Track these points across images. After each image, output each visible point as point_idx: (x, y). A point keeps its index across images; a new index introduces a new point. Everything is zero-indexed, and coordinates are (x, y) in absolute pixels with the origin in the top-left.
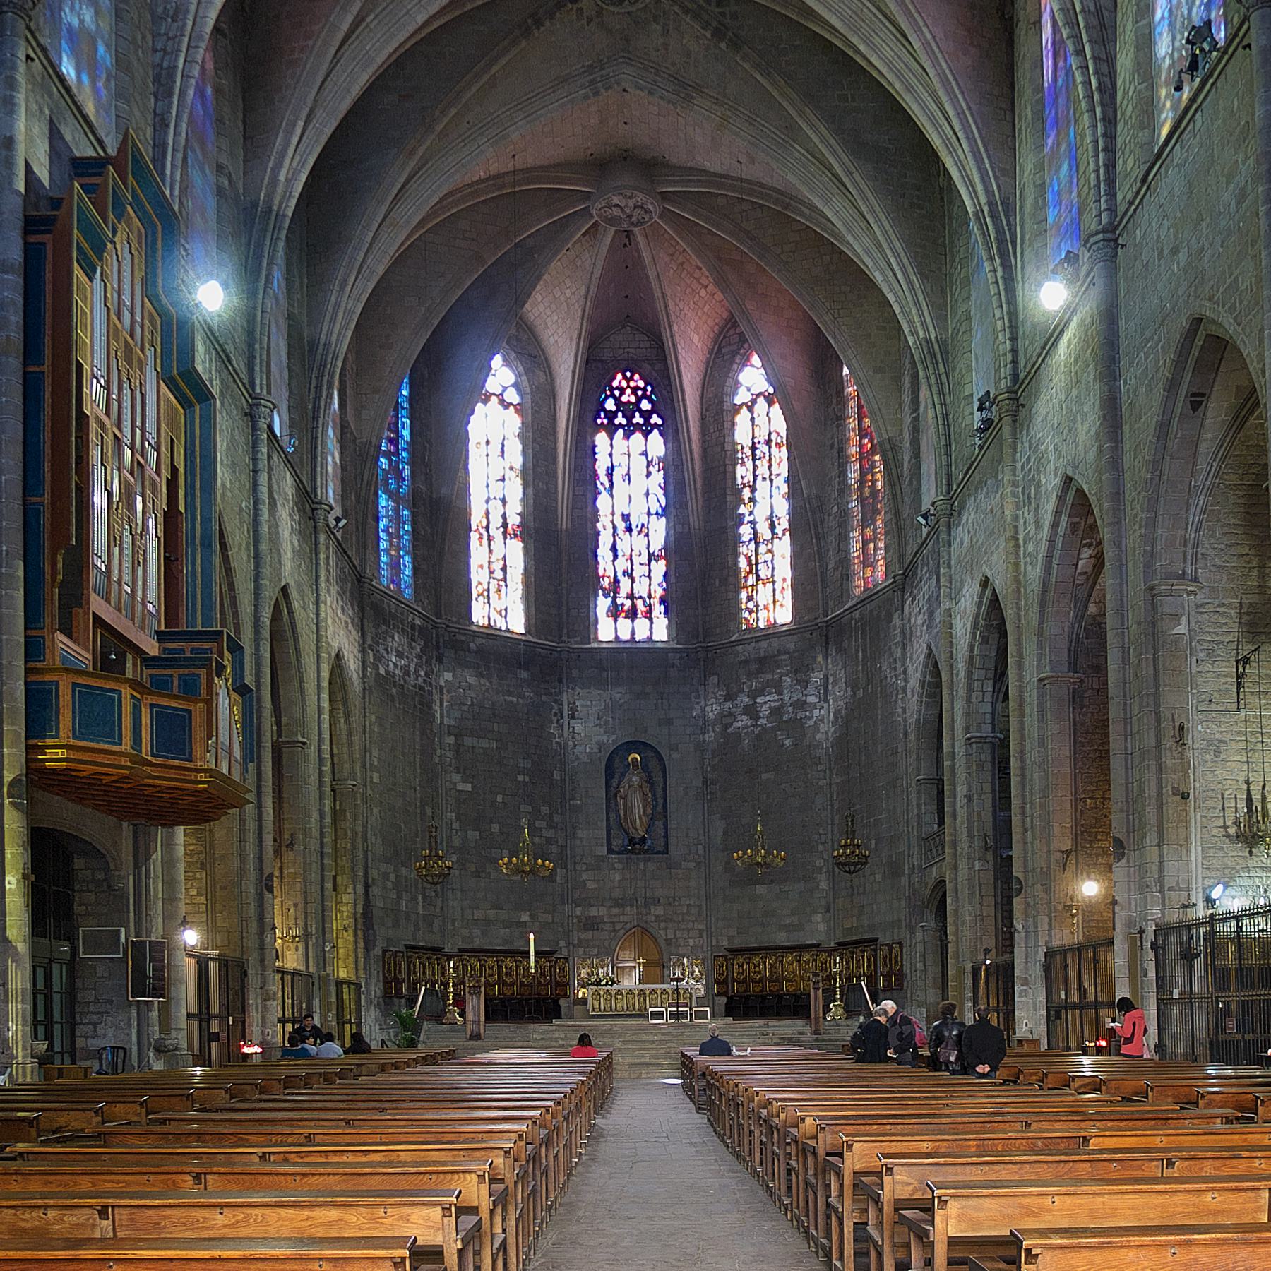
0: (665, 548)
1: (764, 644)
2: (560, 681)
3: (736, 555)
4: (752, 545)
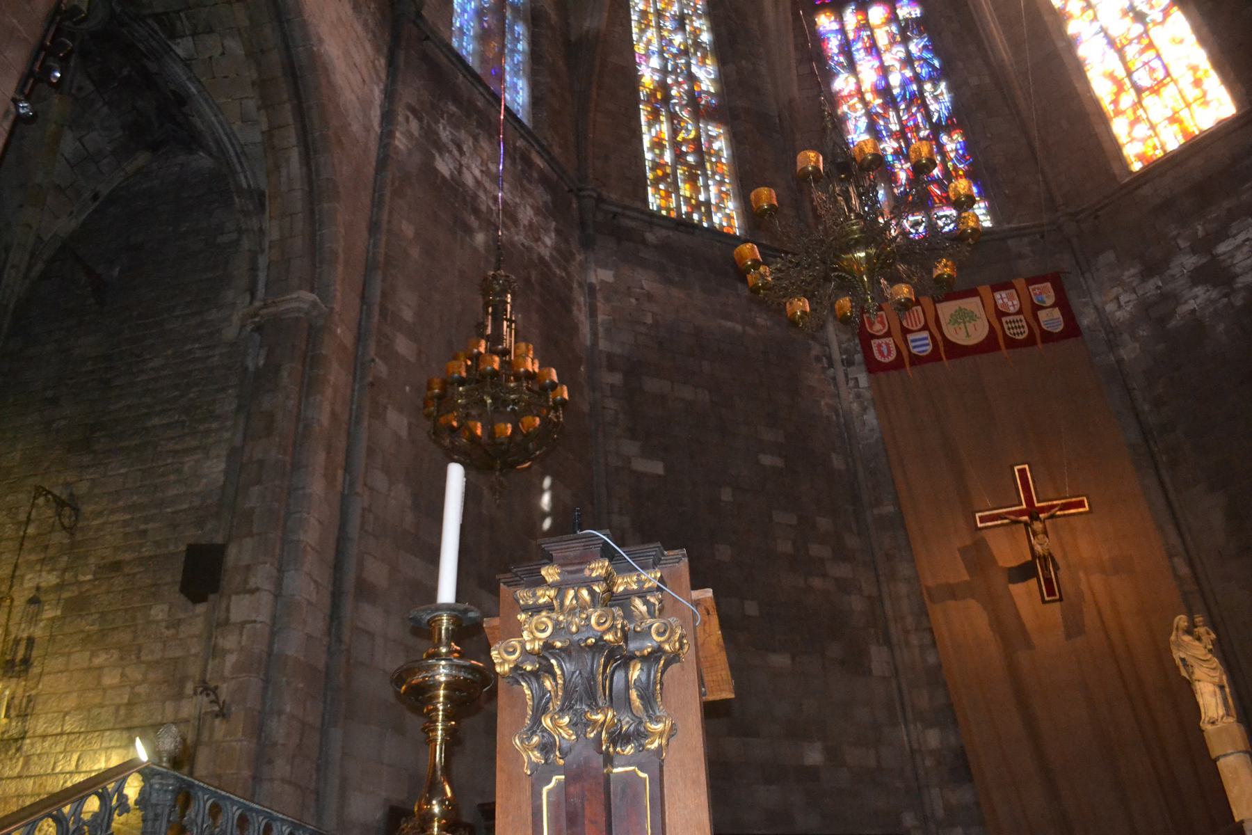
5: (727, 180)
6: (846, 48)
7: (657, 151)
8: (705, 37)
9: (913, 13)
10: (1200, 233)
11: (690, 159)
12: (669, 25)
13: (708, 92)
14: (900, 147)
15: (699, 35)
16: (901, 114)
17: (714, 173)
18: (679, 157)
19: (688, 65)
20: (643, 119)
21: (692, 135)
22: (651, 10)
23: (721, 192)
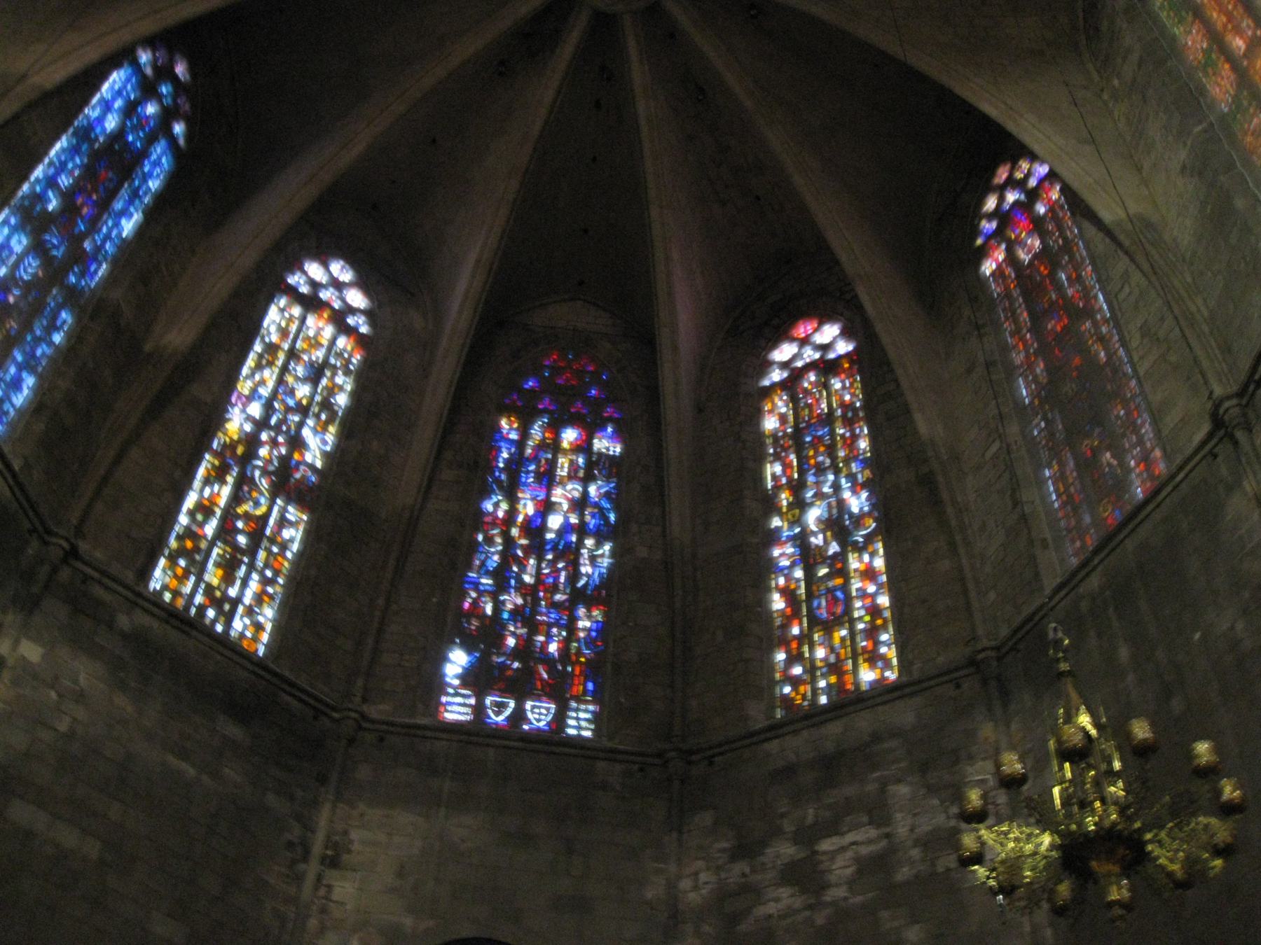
0: (611, 581)
1: (834, 728)
2: (322, 780)
3: (762, 590)
4: (799, 573)
5: (281, 581)
6: (516, 464)
7: (199, 517)
8: (342, 400)
9: (612, 449)
10: (810, 819)
11: (242, 540)
12: (300, 371)
13: (312, 467)
14: (524, 606)
15: (336, 394)
16: (544, 565)
17: (267, 565)
18: (226, 531)
19: (301, 425)
20: (201, 472)
21: (260, 512)
22: (286, 346)
23: (264, 592)
